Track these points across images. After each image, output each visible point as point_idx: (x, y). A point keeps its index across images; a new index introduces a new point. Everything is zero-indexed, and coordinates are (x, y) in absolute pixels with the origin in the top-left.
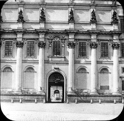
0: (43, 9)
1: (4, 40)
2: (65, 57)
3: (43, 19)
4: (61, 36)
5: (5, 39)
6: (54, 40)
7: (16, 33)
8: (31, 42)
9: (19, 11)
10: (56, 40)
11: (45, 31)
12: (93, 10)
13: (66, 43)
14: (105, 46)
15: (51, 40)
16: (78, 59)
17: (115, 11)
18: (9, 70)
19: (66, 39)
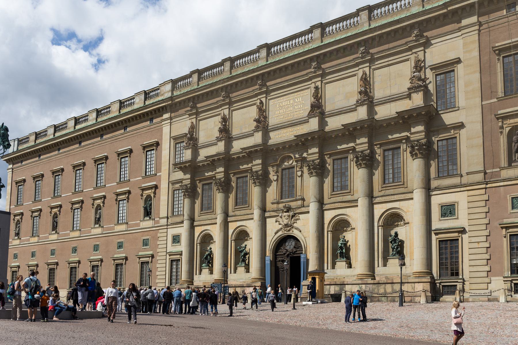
2: (303, 200)
3: (262, 123)
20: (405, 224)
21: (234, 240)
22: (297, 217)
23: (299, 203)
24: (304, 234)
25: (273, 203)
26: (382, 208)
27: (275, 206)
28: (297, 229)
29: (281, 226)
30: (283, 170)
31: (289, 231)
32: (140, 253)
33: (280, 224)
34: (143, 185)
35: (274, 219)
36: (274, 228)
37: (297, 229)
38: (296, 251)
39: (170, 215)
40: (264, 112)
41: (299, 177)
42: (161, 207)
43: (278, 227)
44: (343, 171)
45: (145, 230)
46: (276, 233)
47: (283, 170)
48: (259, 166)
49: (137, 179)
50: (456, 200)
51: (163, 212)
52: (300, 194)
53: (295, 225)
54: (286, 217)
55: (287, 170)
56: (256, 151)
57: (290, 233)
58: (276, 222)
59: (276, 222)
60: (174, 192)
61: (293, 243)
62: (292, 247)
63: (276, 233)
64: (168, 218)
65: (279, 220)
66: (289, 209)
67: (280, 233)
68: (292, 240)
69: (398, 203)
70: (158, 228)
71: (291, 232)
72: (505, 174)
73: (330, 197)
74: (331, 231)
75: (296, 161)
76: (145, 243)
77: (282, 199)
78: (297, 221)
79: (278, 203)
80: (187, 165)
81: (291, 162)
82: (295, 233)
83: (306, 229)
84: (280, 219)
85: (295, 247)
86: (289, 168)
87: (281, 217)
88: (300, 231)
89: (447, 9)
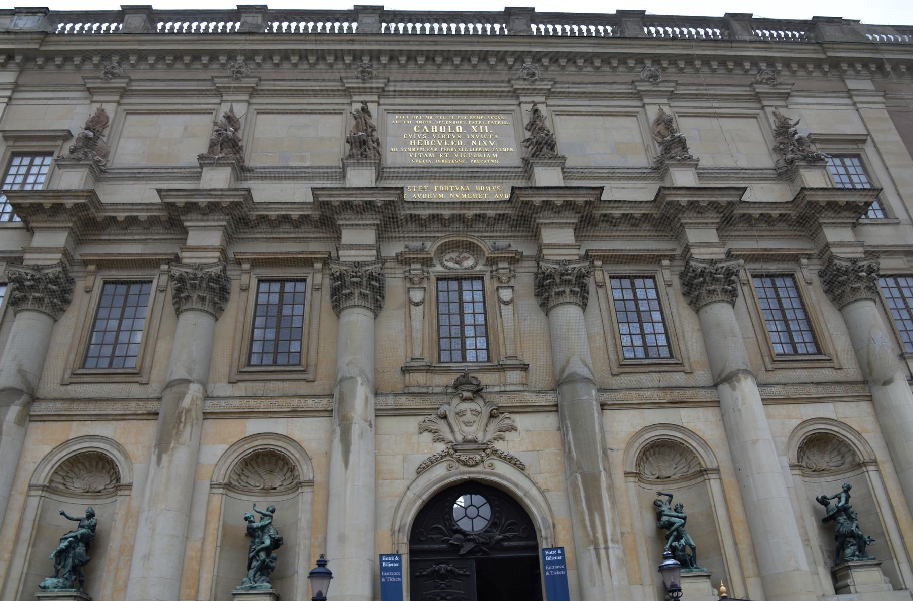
0: (365, 110)
1: (92, 267)
2: (524, 368)
4: (490, 243)
5: (103, 264)
6: (439, 268)
7: (180, 223)
8: (283, 281)
9: (221, 114)
10: (451, 265)
11: (379, 199)
12: (661, 110)
13: (525, 278)
15: (419, 266)
16: (623, 377)
17: (783, 112)
18: (101, 482)
19: (516, 259)
20: (860, 465)
22: (507, 421)
23: (514, 377)
25: (405, 370)
26: (789, 417)
28: (512, 461)
29: (441, 447)
30: (438, 279)
31: (477, 464)
35: (412, 424)
37: (512, 461)
38: (502, 540)
40: (374, 130)
41: (506, 303)
43: (428, 447)
44: (643, 306)
46: (422, 470)
47: (438, 279)
48: (365, 253)
54: (469, 416)
55: (454, 285)
57: (478, 473)
58: (423, 430)
61: (486, 511)
62: (480, 525)
63: (422, 470)
65: (432, 426)
66: (478, 392)
68: (478, 499)
69: (831, 406)
71: (479, 468)
73: (616, 371)
75: (491, 261)
77: (440, 362)
78: (507, 435)
79: (429, 370)
80: (69, 202)
81: (469, 263)
82: (502, 473)
84: (442, 425)
86: (460, 279)
89: (825, 53)
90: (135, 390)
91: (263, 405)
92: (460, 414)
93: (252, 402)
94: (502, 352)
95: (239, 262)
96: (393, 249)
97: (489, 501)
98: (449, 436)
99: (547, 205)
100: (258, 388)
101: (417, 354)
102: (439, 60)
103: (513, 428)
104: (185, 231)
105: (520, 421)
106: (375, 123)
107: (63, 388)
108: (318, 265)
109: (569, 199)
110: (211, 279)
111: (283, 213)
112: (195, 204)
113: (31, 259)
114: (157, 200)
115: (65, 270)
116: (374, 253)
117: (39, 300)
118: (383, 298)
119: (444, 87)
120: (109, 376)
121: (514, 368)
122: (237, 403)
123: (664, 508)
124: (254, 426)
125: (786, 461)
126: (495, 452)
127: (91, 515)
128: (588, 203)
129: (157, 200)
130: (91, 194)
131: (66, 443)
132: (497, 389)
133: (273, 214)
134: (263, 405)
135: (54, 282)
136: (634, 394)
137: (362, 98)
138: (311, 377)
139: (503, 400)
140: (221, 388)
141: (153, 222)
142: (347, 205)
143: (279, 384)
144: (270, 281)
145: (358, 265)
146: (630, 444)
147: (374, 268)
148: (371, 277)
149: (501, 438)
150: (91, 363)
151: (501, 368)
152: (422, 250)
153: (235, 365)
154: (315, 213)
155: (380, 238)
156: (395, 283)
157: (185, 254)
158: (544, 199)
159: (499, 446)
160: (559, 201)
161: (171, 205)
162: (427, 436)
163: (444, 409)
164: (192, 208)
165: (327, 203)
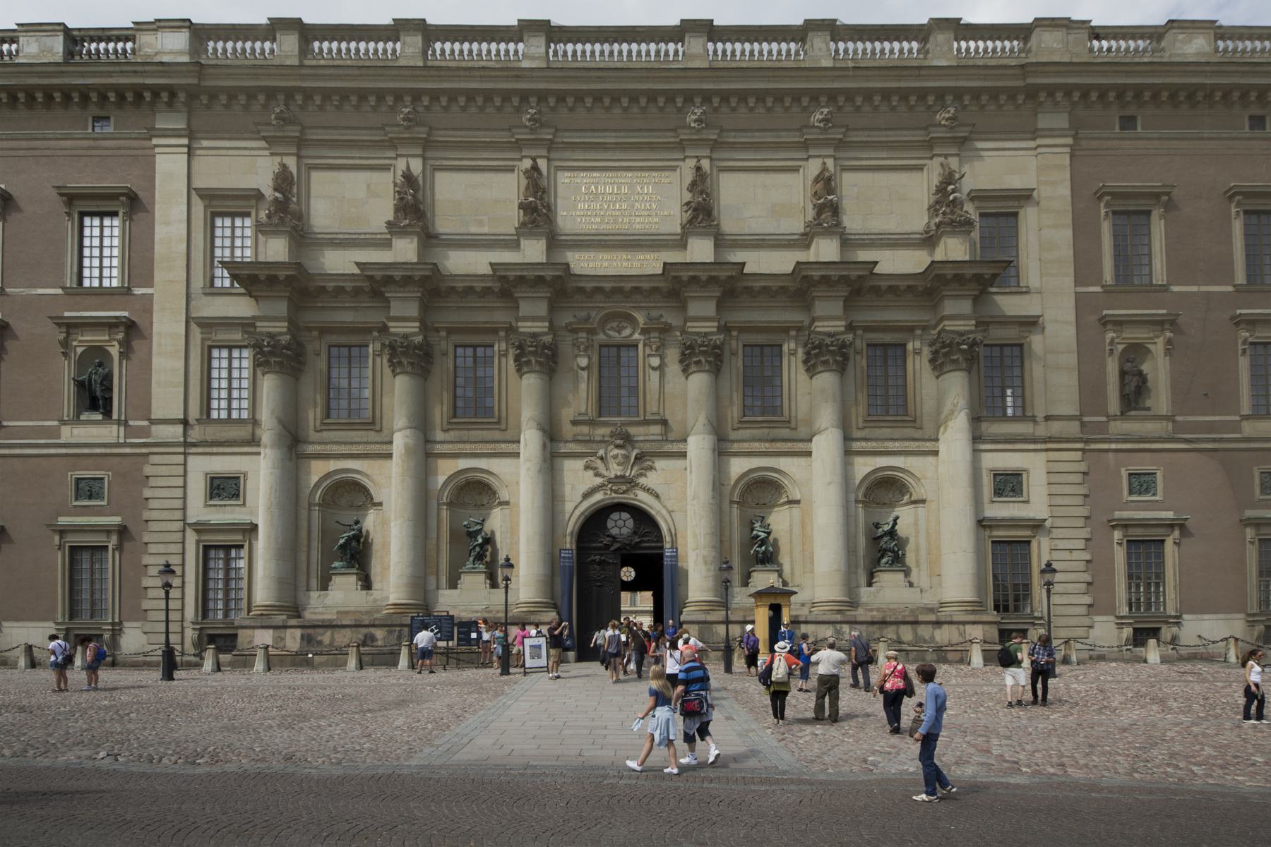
2: (664, 423)
14: (890, 354)
21: (447, 504)
23: (656, 430)
24: (669, 505)
25: (575, 423)
27: (585, 429)
29: (599, 480)
32: (63, 520)
33: (597, 475)
34: (67, 314)
35: (580, 464)
36: (581, 485)
39: (194, 412)
42: (156, 390)
43: (591, 480)
45: (86, 451)
48: (539, 324)
49: (40, 291)
50: (1025, 466)
51: (167, 397)
52: (655, 410)
53: (642, 480)
54: (620, 459)
56: (540, 280)
58: (587, 468)
59: (587, 468)
60: (210, 354)
61: (630, 523)
62: (625, 531)
64: (185, 422)
65: (594, 465)
67: (598, 497)
68: (625, 515)
70: (144, 450)
72: (1119, 427)
74: (738, 503)
76: (87, 489)
77: (600, 416)
78: (649, 474)
79: (592, 423)
80: (282, 274)
83: (683, 500)
85: (635, 533)
87: (602, 458)
88: (657, 496)
90: (372, 436)
91: (468, 448)
92: (615, 457)
93: (461, 446)
94: (648, 409)
95: (437, 330)
96: (566, 318)
97: (632, 517)
98: (605, 472)
99: (694, 279)
100: (464, 434)
101: (583, 410)
102: (607, 101)
103: (651, 468)
104: (387, 300)
105: (660, 464)
106: (545, 183)
107: (318, 434)
108: (502, 334)
109: (714, 274)
110: (415, 347)
111: (468, 284)
112: (391, 277)
113: (263, 327)
114: (356, 271)
115: (294, 337)
116: (547, 324)
117: (280, 364)
118: (555, 363)
119: (610, 139)
120: (350, 426)
121: (655, 422)
122: (450, 446)
123: (757, 525)
124: (463, 464)
125: (852, 497)
126: (637, 485)
127: (357, 522)
128: (730, 277)
129: (356, 271)
130: (299, 266)
131: (329, 475)
132: (641, 438)
133: (460, 285)
134: (468, 448)
135: (287, 347)
136: (746, 445)
137: (534, 153)
138: (503, 426)
139: (647, 447)
140: (440, 436)
141: (357, 292)
142: (521, 279)
143: (480, 432)
144: (465, 346)
145: (534, 335)
146: (737, 481)
147: (548, 339)
148: (544, 347)
149: (641, 475)
150: (334, 413)
151: (647, 423)
152: (587, 319)
153: (445, 416)
154: (496, 286)
155: (552, 308)
156: (566, 346)
157: (390, 324)
158: (691, 274)
159: (642, 480)
160: (704, 276)
161: (370, 278)
162: (591, 473)
163: (601, 452)
164: (388, 280)
165: (505, 277)
